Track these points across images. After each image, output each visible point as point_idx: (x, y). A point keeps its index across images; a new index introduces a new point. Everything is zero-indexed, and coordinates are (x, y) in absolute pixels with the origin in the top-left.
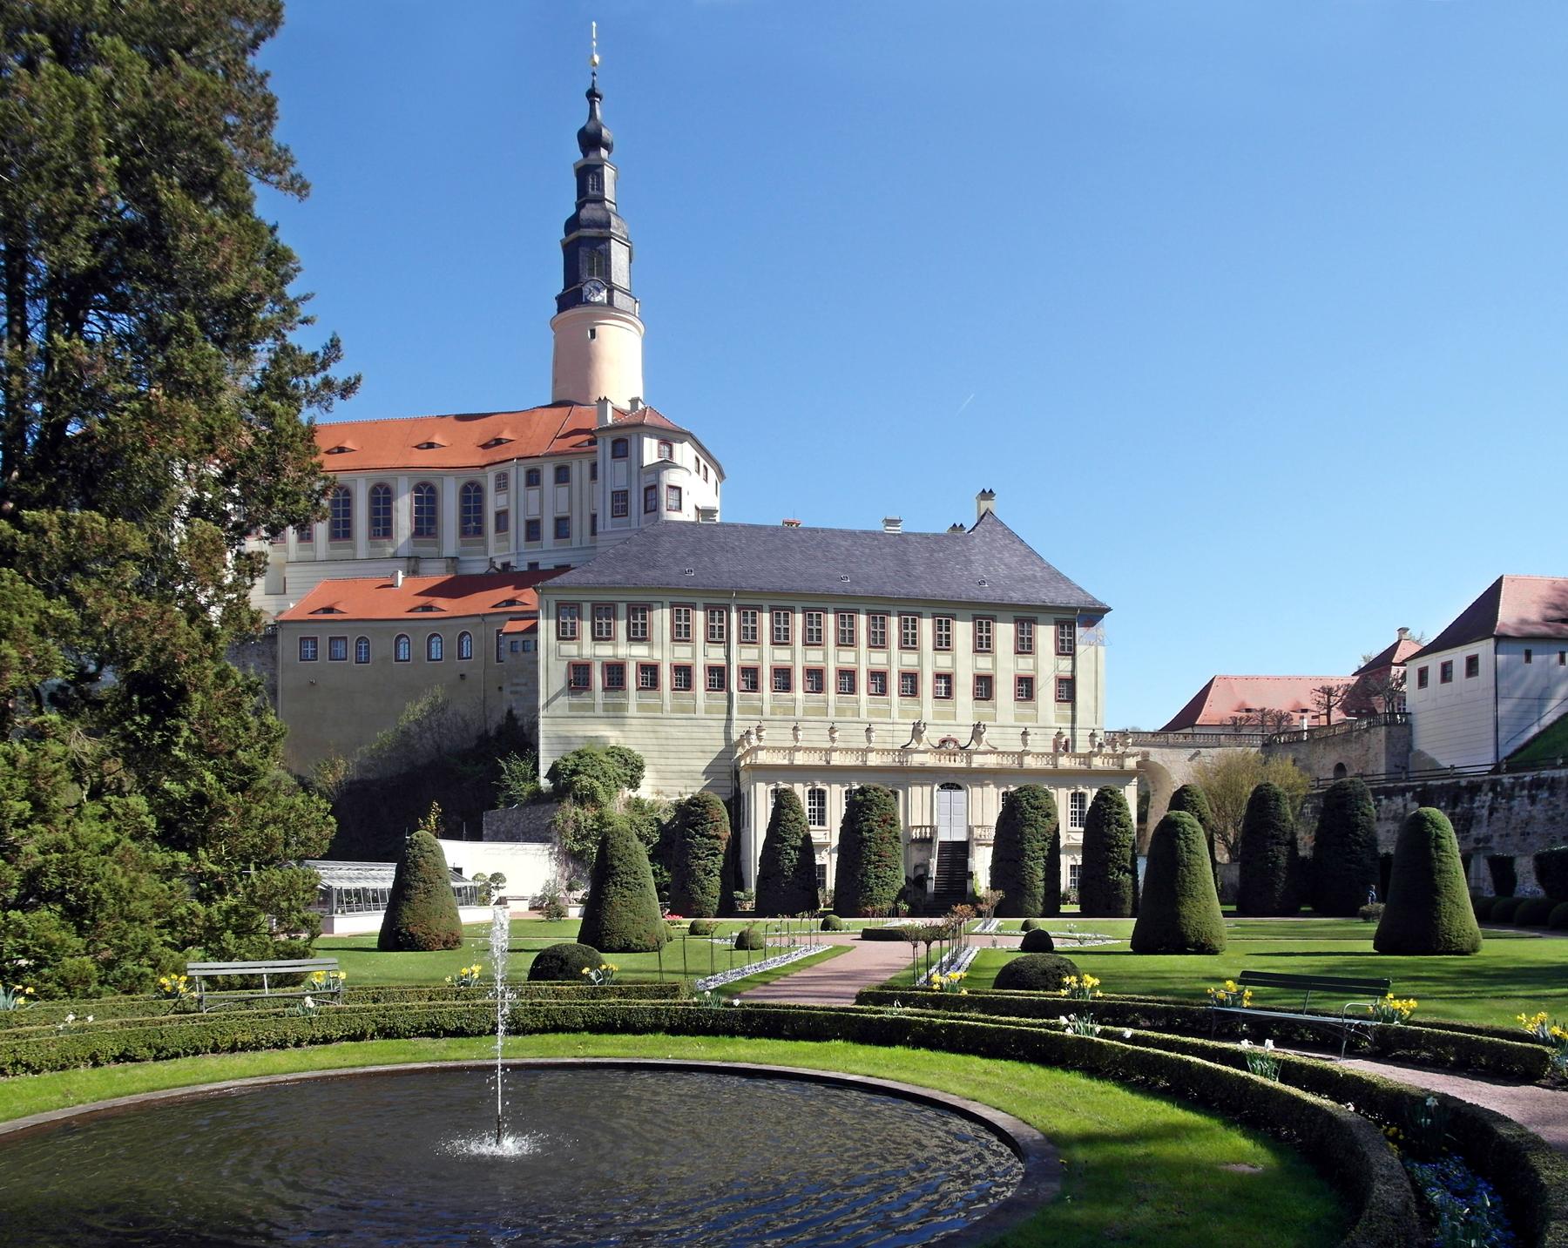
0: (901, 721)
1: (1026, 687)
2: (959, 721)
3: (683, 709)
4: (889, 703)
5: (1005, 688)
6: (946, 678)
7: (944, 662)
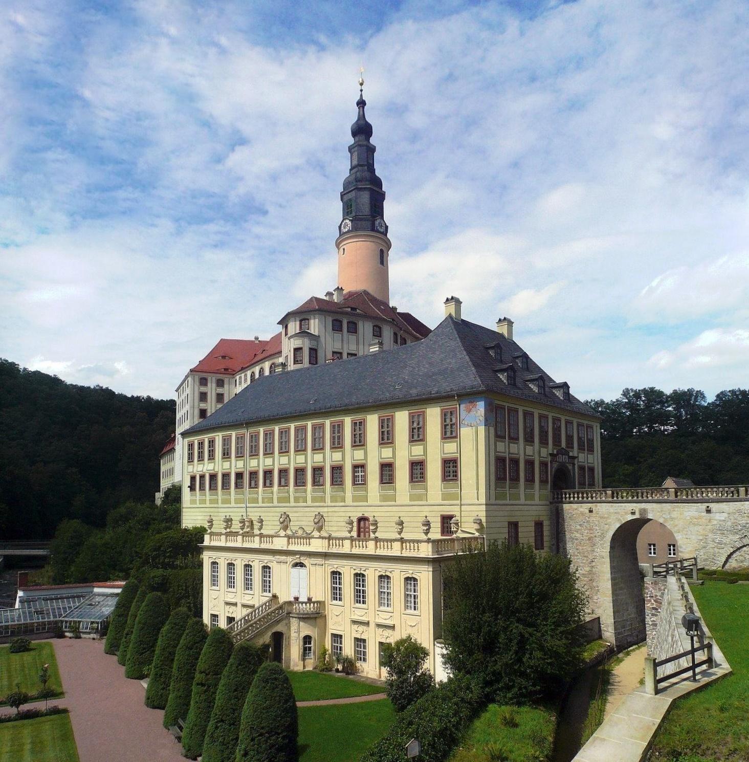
0: (333, 504)
1: (417, 469)
2: (370, 503)
3: (224, 502)
4: (324, 492)
5: (402, 473)
6: (359, 467)
7: (359, 455)
